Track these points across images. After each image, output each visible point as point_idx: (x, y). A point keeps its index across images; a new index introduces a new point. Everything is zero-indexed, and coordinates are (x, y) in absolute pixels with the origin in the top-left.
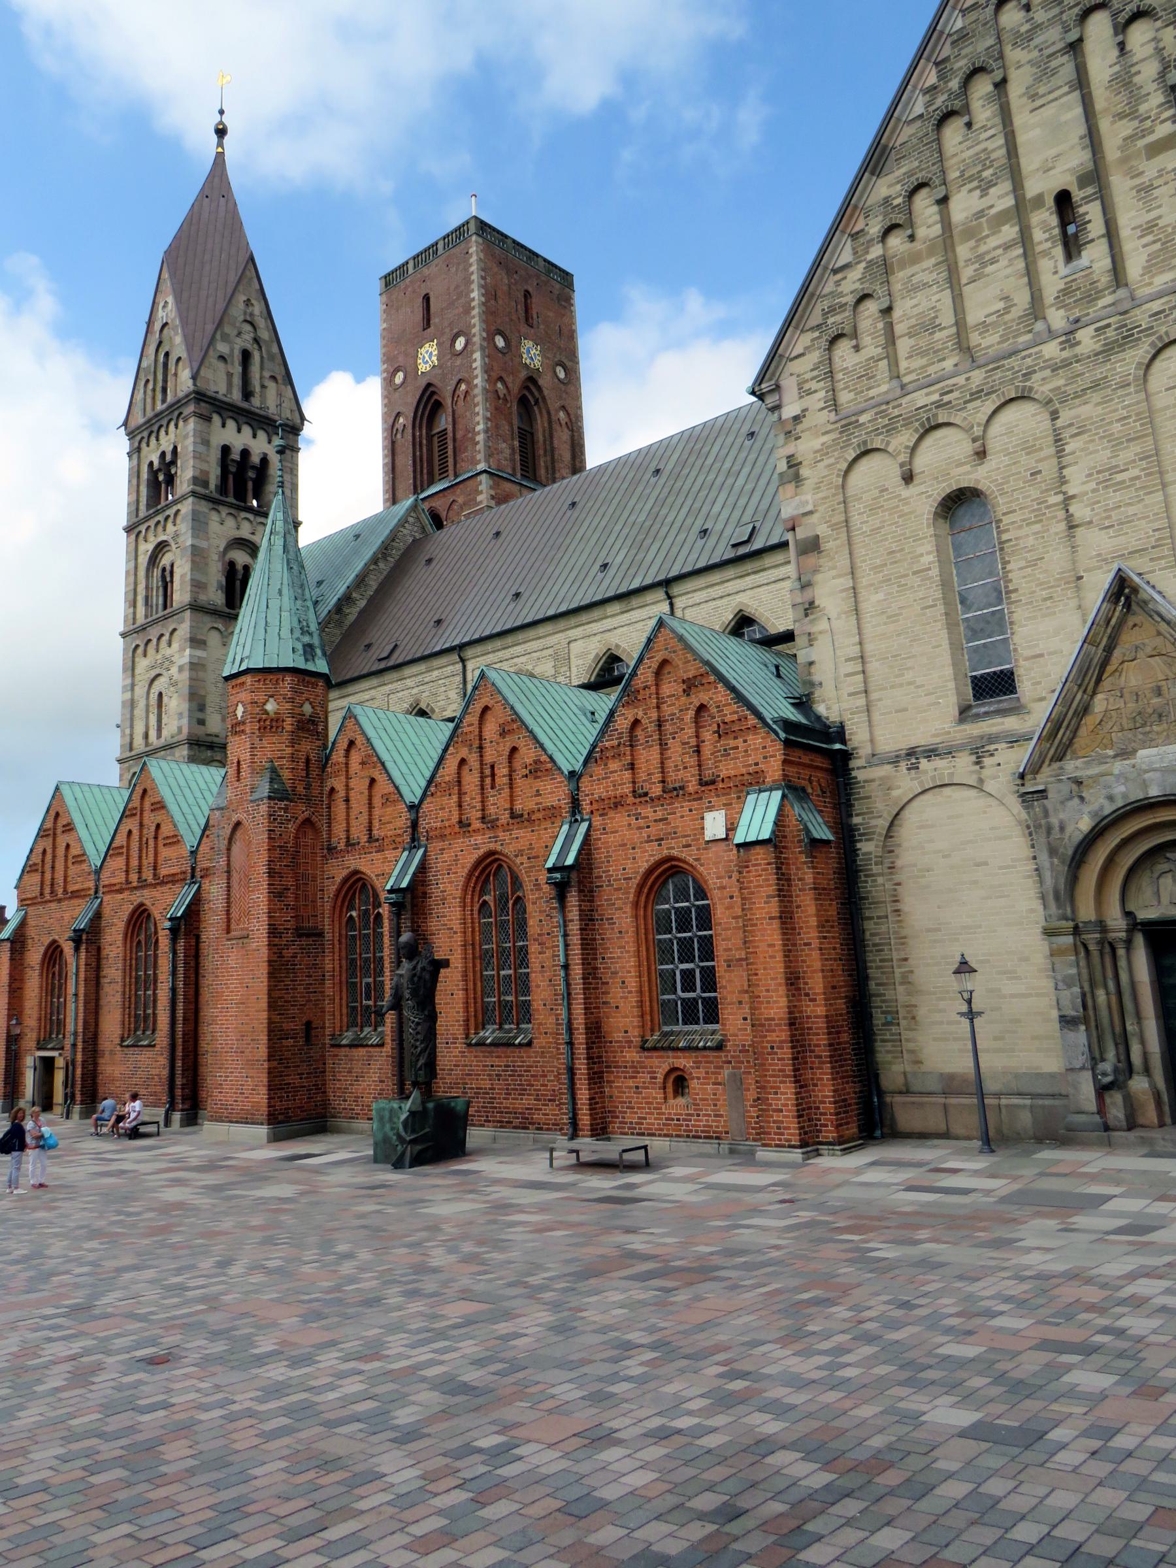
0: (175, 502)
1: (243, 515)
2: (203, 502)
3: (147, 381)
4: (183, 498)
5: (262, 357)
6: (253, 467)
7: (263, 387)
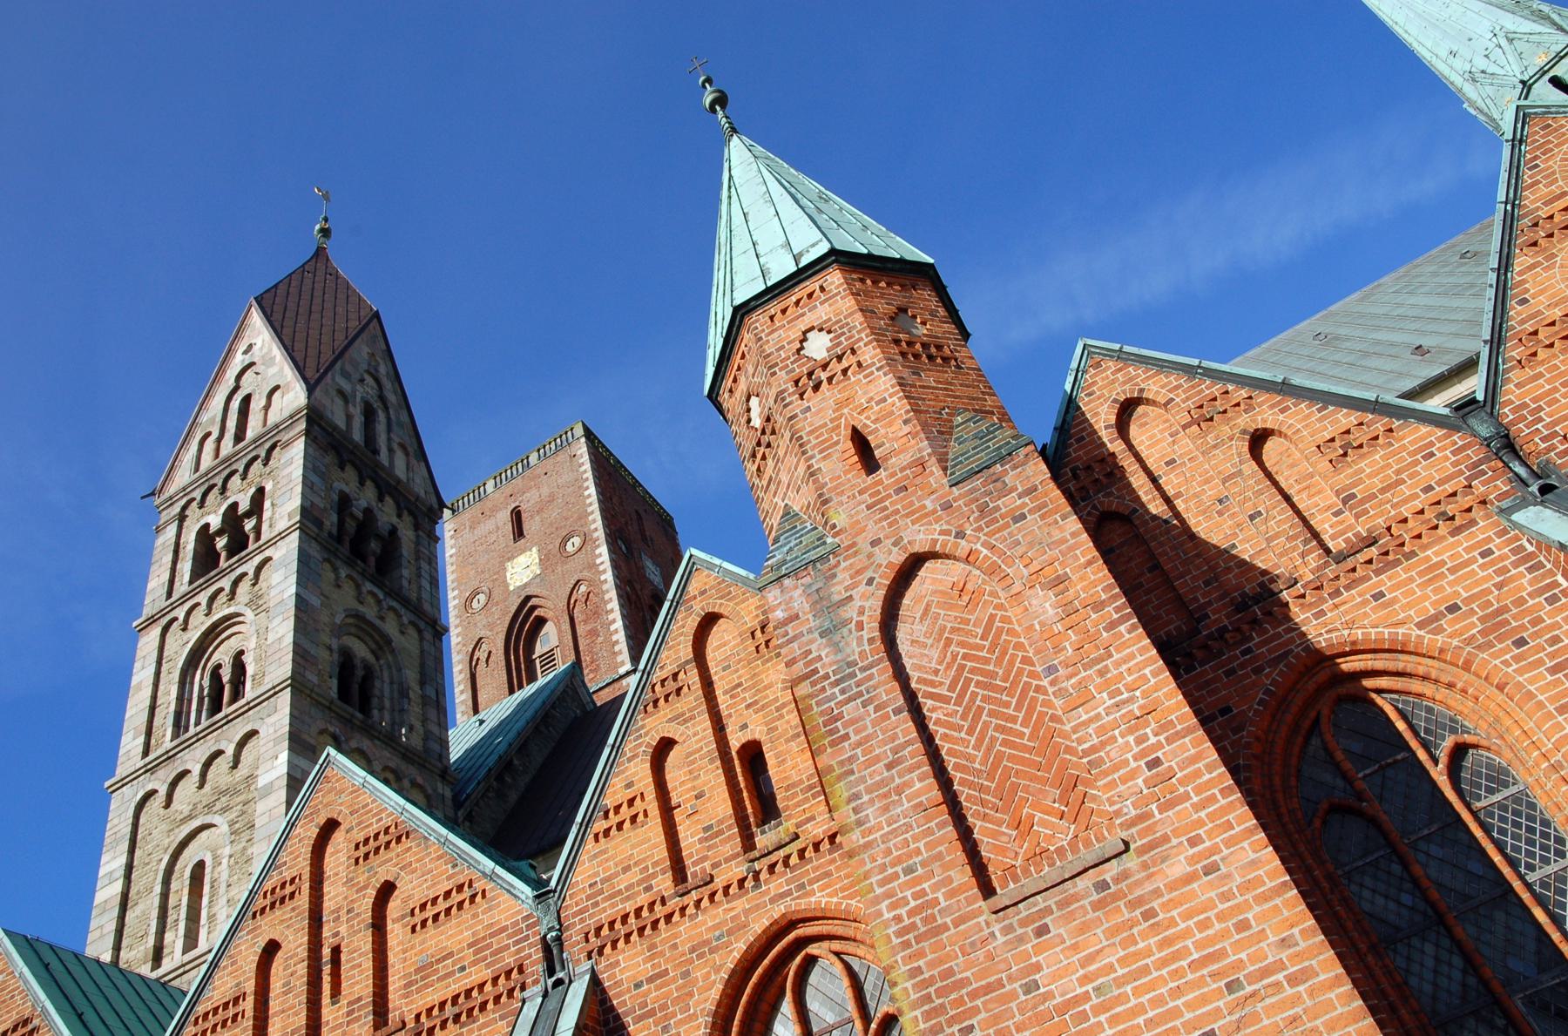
0: (260, 550)
1: (368, 586)
2: (314, 544)
3: (208, 434)
4: (282, 536)
5: (389, 419)
6: (379, 537)
7: (391, 450)
